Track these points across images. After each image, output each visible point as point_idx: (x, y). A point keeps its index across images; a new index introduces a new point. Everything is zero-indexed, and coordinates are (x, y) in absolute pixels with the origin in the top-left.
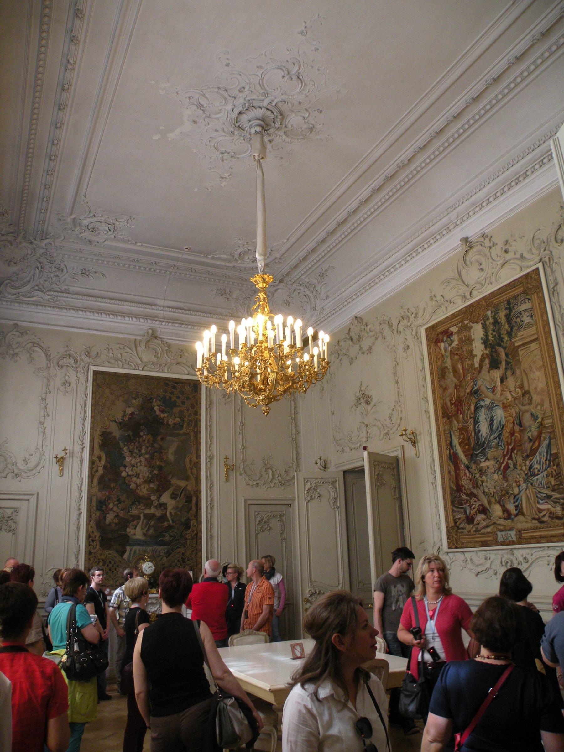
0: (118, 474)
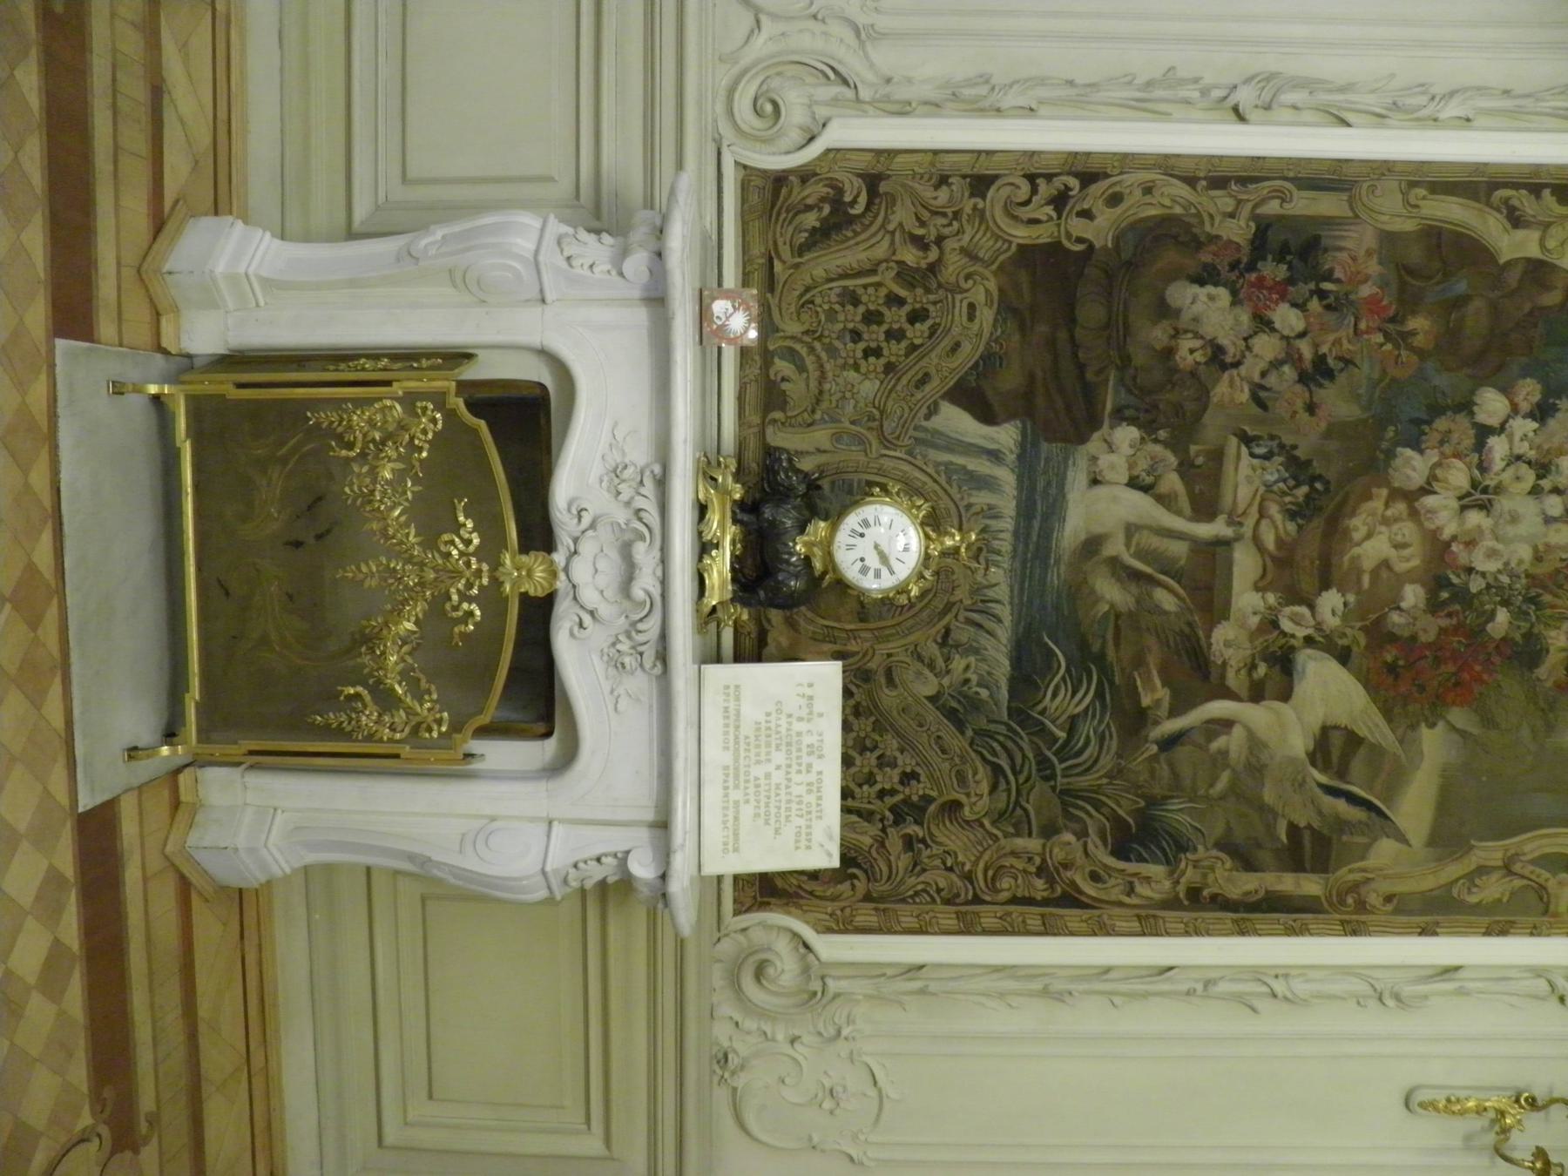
0: (1491, 361)
